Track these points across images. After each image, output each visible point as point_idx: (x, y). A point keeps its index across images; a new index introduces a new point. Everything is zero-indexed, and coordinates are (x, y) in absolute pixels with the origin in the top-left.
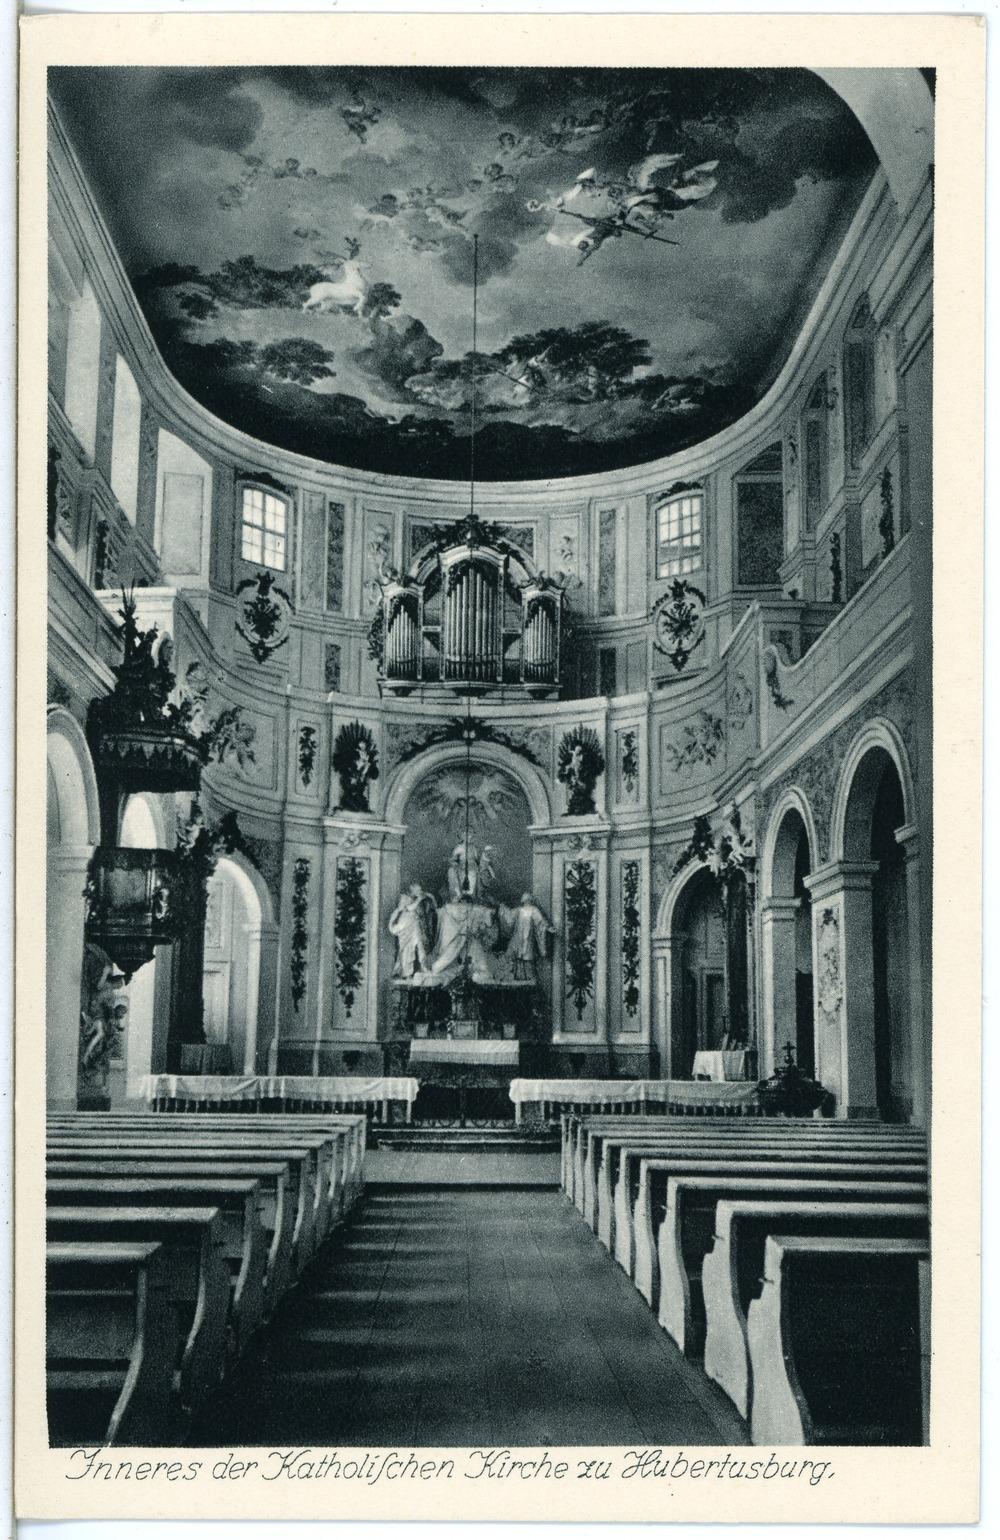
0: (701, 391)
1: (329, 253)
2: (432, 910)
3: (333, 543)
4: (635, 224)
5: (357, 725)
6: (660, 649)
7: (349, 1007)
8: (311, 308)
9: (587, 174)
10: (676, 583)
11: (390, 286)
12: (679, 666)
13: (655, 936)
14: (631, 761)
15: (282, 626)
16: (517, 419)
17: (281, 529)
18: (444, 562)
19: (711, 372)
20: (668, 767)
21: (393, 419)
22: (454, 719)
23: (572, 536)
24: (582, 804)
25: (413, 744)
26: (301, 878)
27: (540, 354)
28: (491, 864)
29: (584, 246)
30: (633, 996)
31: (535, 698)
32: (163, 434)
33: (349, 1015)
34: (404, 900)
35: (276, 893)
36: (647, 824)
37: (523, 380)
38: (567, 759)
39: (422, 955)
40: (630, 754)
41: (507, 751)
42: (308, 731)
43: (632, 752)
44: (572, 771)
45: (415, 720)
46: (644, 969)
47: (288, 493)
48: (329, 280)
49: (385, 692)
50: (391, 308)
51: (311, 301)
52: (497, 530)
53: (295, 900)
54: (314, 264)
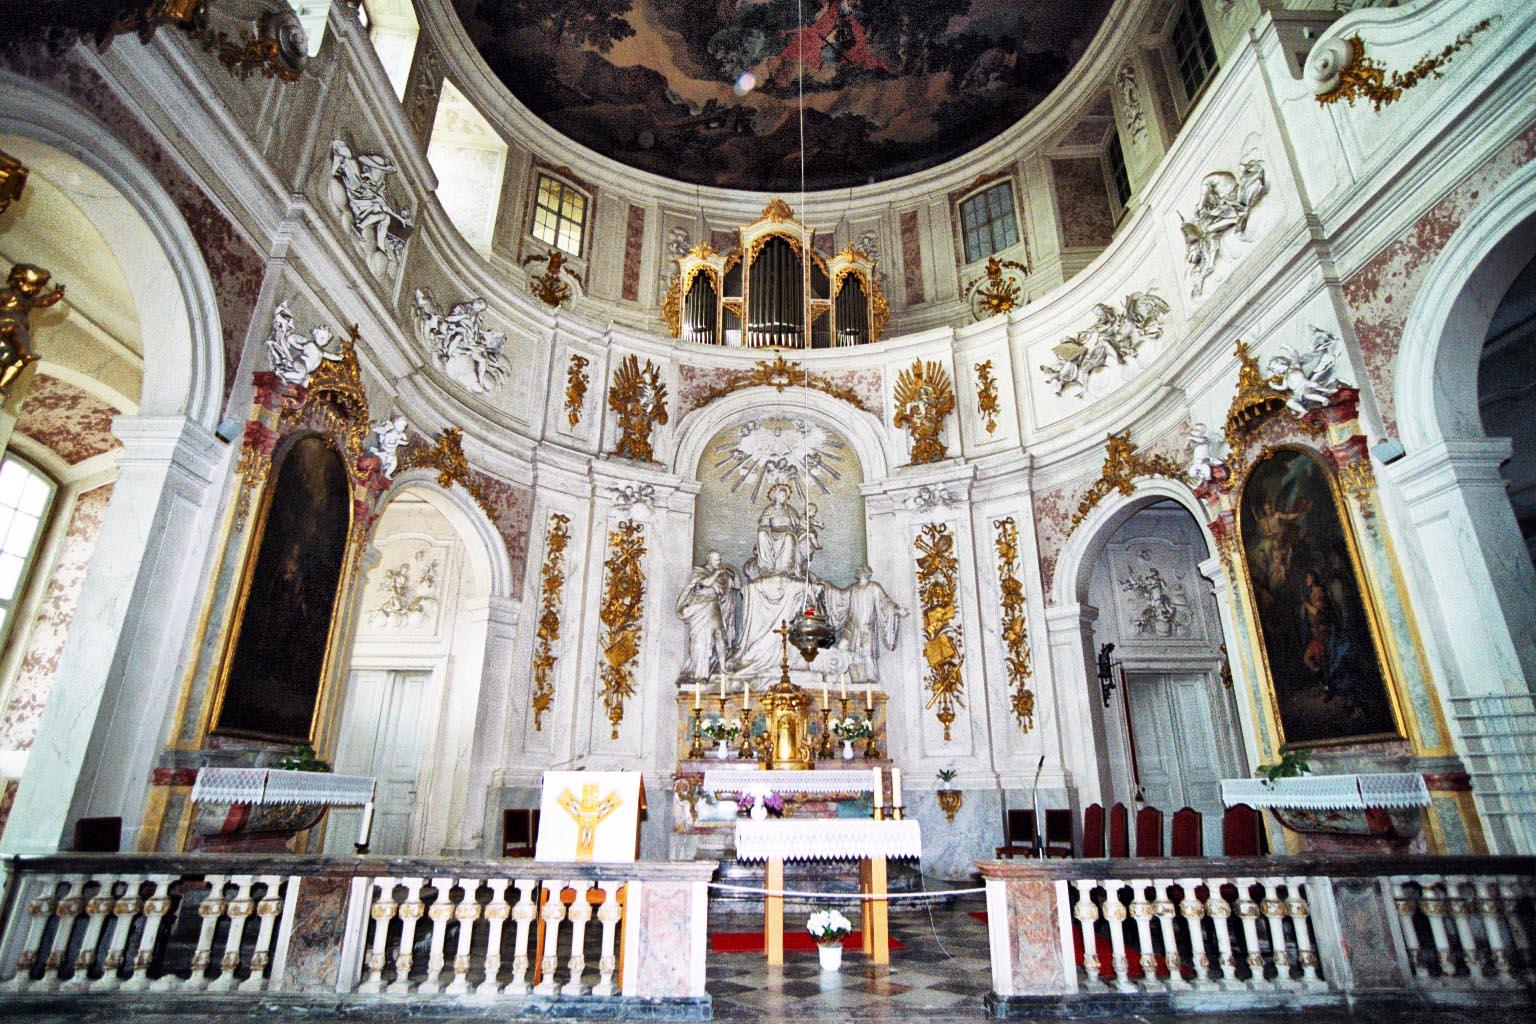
22: (762, 363)
24: (929, 451)
26: (558, 541)
30: (1024, 703)
33: (615, 734)
39: (720, 646)
42: (580, 362)
46: (1039, 665)
53: (546, 570)
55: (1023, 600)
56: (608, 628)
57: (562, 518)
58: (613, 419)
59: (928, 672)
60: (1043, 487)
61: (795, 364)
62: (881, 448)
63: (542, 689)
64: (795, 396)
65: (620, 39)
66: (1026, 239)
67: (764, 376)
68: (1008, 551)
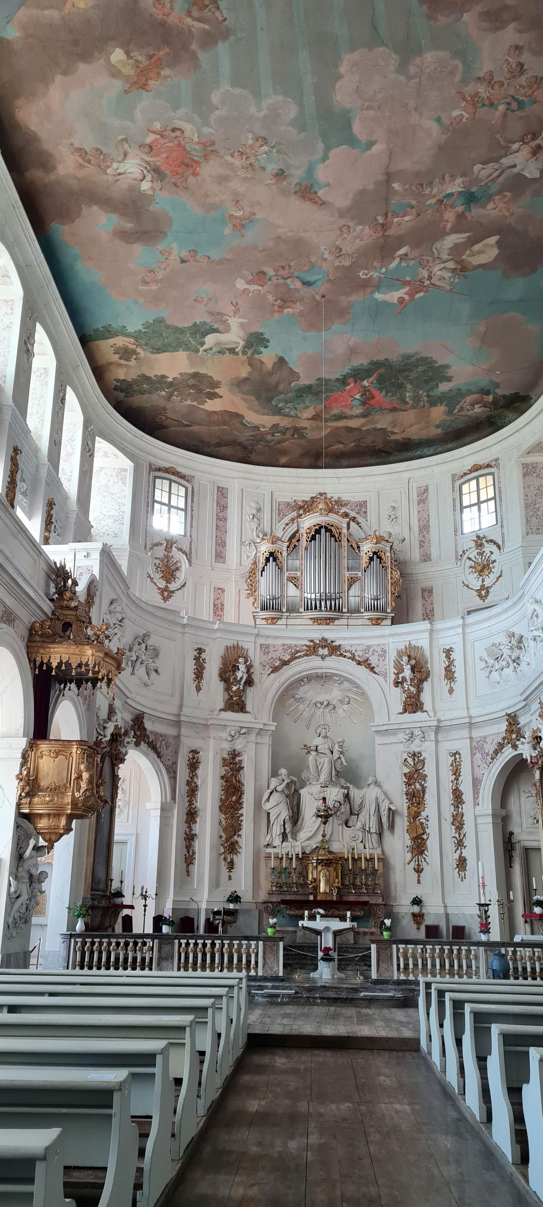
0: (490, 398)
1: (218, 314)
2: (296, 791)
3: (220, 515)
4: (438, 283)
5: (238, 645)
6: (467, 586)
7: (230, 871)
8: (205, 351)
9: (402, 251)
10: (478, 537)
11: (262, 334)
12: (483, 598)
13: (477, 813)
14: (451, 671)
15: (181, 576)
16: (353, 423)
17: (182, 505)
18: (301, 525)
19: (497, 385)
20: (482, 675)
21: (264, 426)
22: (312, 641)
23: (396, 506)
24: (413, 705)
25: (280, 660)
26: (194, 765)
27: (370, 377)
28: (341, 753)
29: (401, 300)
30: (462, 863)
31: (374, 625)
32: (97, 438)
33: (230, 878)
34: (274, 782)
35: (173, 777)
36: (467, 720)
37: (357, 396)
38: (400, 669)
39: (288, 826)
40: (449, 666)
41: (354, 663)
42: (200, 651)
43: (451, 663)
44: (404, 679)
45: (280, 642)
46: (470, 841)
47: (188, 481)
48: (219, 332)
49: (259, 621)
50: (262, 349)
51: (204, 348)
52: (339, 503)
53: (188, 783)
54: (208, 321)
55: (464, 803)
56: (223, 816)
57: (195, 752)
58: (221, 685)
59: (409, 843)
60: (477, 734)
61: (332, 642)
62: (385, 697)
63: (189, 852)
64: (333, 664)
65: (212, 399)
66: (502, 522)
67: (313, 649)
68: (457, 773)
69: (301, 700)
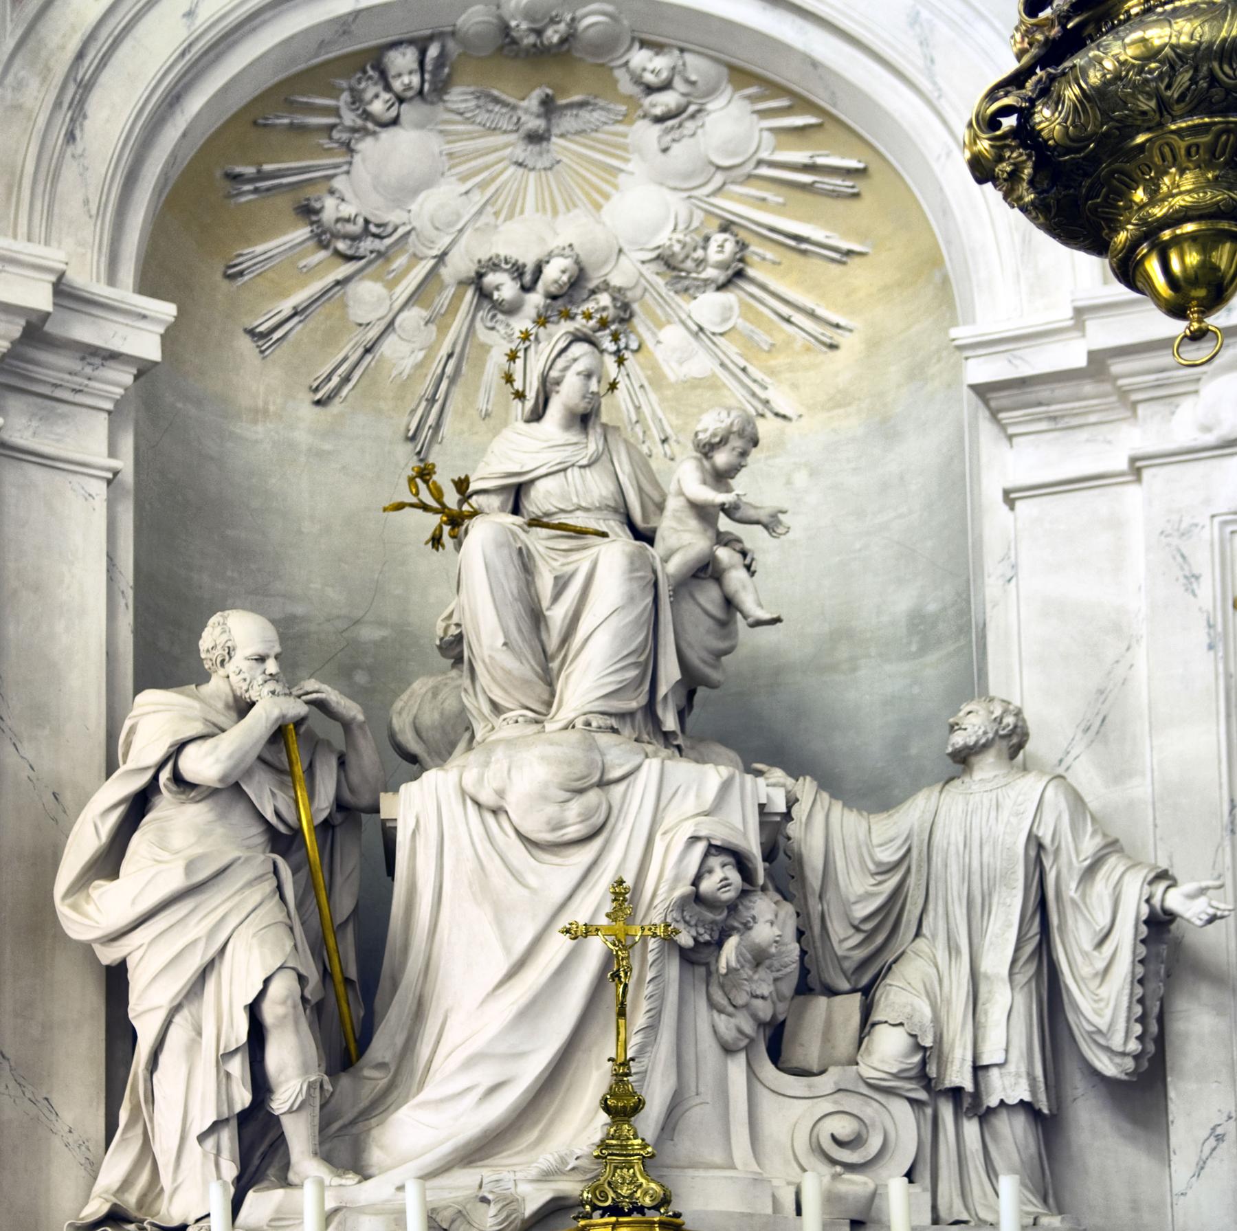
69: (363, 246)
